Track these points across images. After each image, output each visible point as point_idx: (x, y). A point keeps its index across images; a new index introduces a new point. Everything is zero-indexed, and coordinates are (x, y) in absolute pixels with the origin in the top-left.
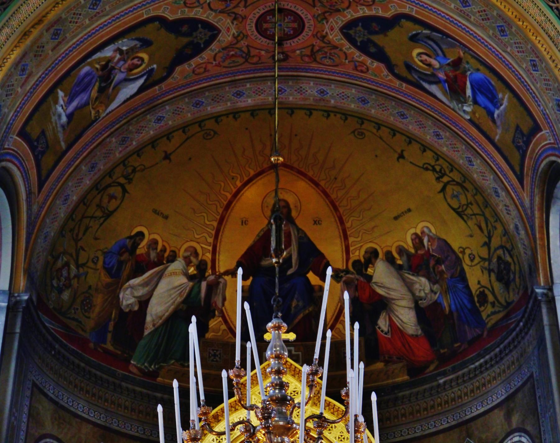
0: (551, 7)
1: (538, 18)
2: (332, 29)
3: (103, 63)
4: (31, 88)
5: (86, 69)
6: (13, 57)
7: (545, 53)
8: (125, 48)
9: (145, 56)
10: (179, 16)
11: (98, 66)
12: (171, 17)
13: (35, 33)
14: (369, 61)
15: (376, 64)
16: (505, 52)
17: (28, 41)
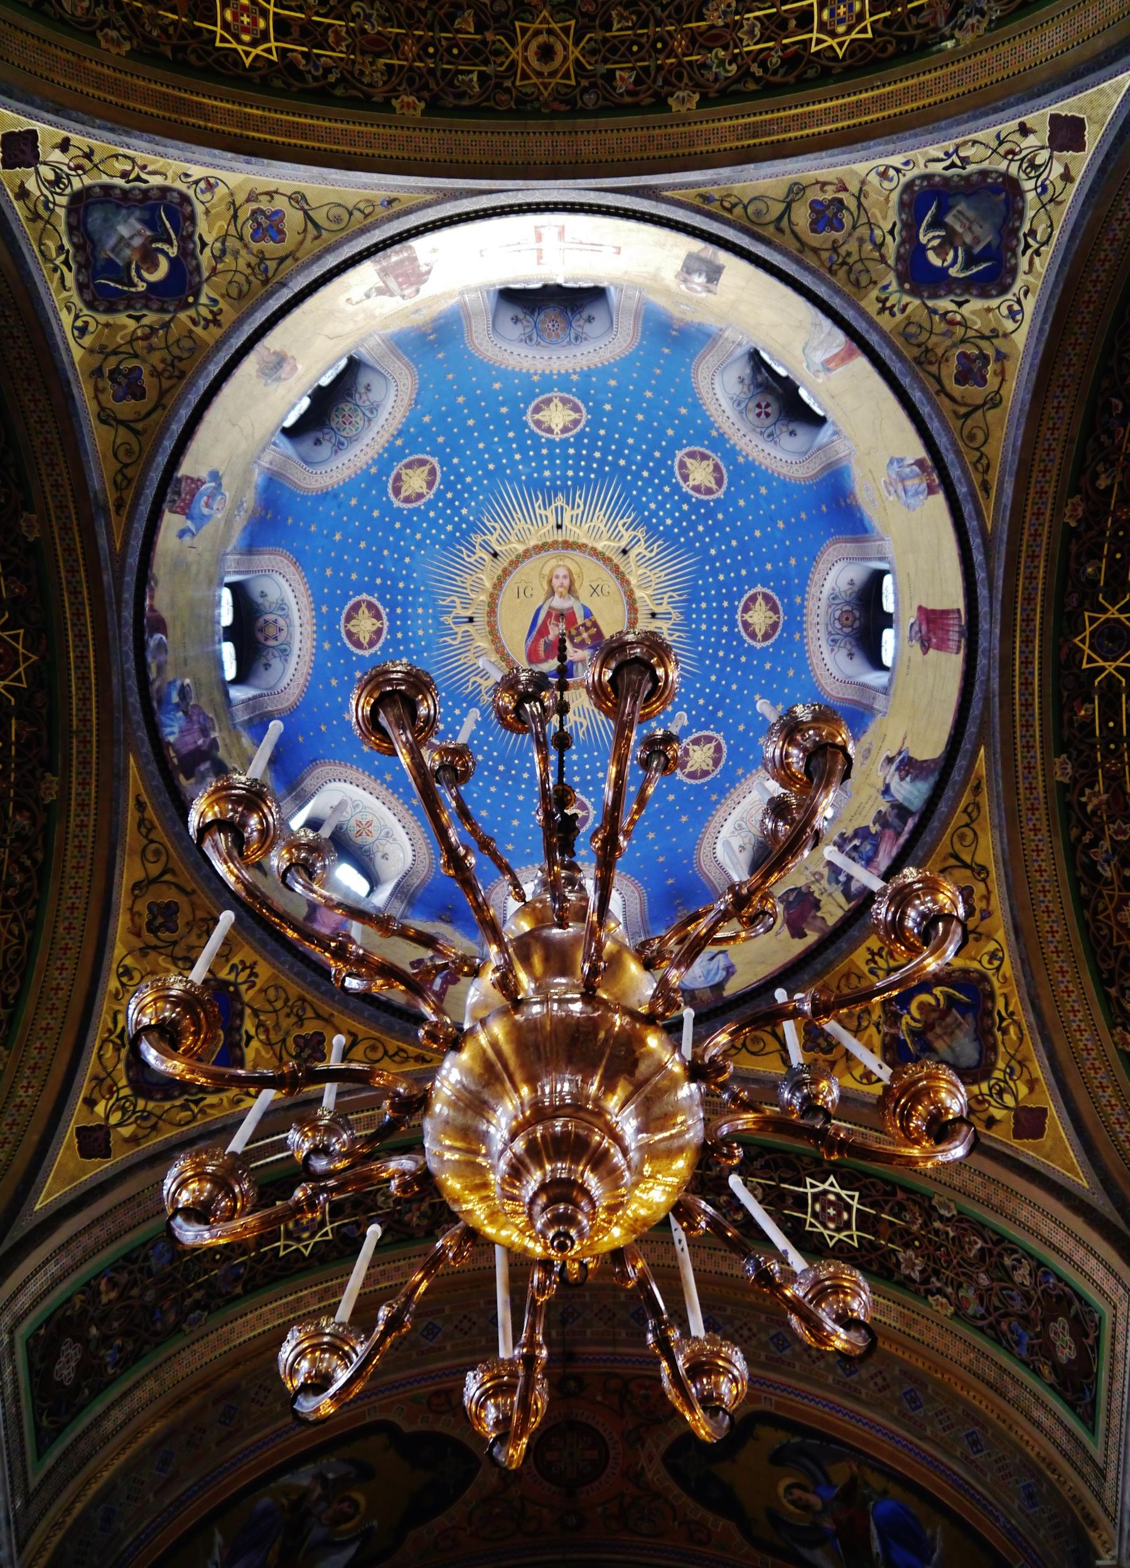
0: (981, 1329)
1: (965, 1359)
2: (650, 1459)
3: (294, 1497)
4: (170, 1505)
5: (265, 1501)
6: (152, 1430)
7: (988, 1412)
8: (331, 1476)
9: (360, 1498)
10: (419, 1426)
11: (284, 1501)
12: (407, 1428)
13: (195, 1401)
14: (710, 1517)
15: (722, 1522)
16: (924, 1438)
17: (182, 1412)
